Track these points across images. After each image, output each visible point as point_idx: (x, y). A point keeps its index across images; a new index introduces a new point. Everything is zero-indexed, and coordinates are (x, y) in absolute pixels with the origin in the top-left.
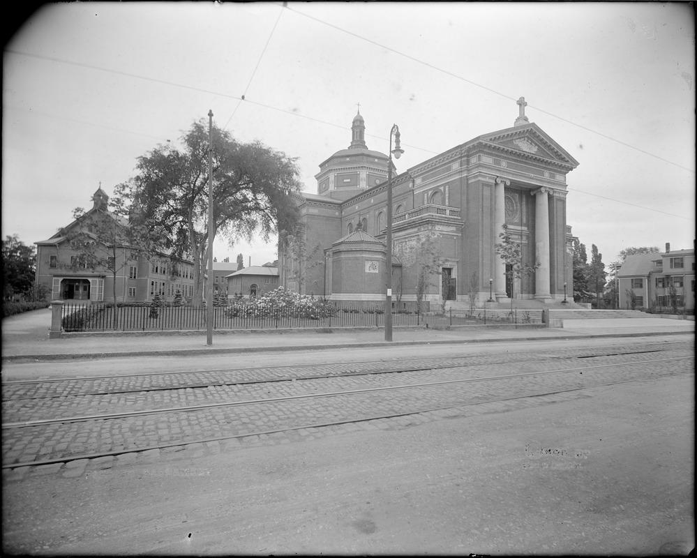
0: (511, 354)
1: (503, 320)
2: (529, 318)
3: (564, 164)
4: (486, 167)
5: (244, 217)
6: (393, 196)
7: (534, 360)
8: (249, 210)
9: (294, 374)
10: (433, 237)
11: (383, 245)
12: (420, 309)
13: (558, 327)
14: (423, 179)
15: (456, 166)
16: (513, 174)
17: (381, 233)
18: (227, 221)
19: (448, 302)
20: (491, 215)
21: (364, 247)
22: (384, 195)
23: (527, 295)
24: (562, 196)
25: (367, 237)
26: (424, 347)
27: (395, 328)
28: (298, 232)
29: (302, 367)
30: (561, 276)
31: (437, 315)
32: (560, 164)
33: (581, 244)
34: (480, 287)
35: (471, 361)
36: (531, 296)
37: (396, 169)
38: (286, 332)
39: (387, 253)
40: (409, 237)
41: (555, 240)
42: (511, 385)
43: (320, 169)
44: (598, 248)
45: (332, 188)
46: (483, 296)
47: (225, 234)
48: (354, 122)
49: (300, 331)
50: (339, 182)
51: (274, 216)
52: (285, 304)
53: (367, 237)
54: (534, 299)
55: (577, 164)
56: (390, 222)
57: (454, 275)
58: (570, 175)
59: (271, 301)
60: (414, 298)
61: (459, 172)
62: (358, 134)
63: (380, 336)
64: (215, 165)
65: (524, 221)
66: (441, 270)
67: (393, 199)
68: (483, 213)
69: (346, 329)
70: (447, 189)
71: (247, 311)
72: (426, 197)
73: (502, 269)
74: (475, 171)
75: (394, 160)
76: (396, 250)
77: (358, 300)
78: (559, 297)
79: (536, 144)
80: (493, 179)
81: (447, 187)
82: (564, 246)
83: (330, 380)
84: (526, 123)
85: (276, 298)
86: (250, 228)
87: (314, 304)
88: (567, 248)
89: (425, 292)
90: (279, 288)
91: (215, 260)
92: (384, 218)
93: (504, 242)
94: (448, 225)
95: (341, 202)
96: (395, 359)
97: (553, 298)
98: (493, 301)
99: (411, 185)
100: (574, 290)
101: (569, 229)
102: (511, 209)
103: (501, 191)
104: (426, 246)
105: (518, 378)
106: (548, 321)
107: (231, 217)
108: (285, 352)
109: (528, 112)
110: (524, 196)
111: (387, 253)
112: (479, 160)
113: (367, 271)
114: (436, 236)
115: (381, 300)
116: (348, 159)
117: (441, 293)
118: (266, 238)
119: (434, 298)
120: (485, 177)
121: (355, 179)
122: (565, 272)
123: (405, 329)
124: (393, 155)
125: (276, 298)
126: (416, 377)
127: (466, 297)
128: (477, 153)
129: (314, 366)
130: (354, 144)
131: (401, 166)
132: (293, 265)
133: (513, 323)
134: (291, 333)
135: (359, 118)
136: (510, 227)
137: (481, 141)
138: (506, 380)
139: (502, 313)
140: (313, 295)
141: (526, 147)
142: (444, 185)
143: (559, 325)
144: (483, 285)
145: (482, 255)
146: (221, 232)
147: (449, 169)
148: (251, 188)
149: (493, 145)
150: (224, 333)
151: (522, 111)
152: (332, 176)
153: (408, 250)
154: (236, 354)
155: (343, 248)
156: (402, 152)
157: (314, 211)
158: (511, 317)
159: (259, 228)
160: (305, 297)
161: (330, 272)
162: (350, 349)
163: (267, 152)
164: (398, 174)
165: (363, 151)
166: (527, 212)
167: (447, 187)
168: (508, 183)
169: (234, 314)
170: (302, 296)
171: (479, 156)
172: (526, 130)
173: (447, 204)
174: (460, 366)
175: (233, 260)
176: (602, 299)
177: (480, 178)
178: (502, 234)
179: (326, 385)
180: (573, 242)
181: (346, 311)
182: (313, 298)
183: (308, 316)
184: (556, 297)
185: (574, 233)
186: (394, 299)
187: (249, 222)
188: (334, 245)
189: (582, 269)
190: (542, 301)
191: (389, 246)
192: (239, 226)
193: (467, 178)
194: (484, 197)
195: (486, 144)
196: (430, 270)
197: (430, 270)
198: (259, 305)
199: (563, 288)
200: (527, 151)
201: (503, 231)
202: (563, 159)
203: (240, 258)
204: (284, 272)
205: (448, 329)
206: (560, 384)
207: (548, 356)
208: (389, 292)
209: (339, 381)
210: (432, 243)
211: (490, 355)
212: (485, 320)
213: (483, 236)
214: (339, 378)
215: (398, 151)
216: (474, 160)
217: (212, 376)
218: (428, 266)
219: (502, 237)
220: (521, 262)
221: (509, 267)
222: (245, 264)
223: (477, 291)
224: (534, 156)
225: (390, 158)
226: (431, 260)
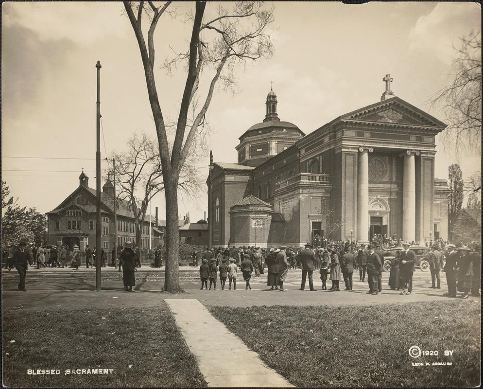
43: (240, 141)
48: (267, 98)
65: (394, 180)
80: (356, 149)
81: (321, 156)
103: (365, 157)
109: (393, 87)
121: (266, 148)
135: (272, 94)
137: (342, 120)
142: (319, 155)
147: (322, 142)
167: (321, 156)
168: (371, 151)
171: (343, 131)
194: (347, 164)
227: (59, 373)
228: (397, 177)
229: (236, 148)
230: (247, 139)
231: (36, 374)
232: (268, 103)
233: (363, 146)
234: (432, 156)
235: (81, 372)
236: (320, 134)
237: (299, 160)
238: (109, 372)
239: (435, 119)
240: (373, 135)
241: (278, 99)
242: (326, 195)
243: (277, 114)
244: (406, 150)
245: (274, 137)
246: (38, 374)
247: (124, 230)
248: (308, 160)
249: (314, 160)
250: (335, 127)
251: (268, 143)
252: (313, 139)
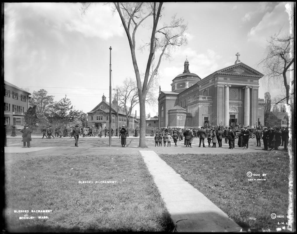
43: (172, 82)
48: (185, 63)
65: (240, 99)
70: (208, 89)
80: (223, 85)
94: (207, 102)
99: (198, 88)
103: (228, 89)
110: (240, 89)
116: (181, 78)
120: (220, 85)
121: (184, 84)
128: (217, 76)
145: (219, 112)
147: (209, 82)
152: (176, 85)
168: (230, 86)
171: (218, 78)
173: (208, 95)
224: (242, 75)
230: (176, 81)
232: (185, 65)
233: (227, 84)
237: (198, 90)
239: (259, 72)
243: (189, 70)
248: (203, 90)
249: (205, 90)
250: (214, 76)
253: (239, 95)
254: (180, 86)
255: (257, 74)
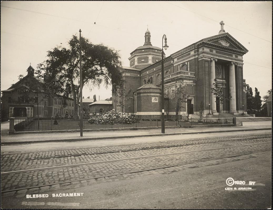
0: (219, 138)
1: (215, 123)
2: (227, 122)
3: (242, 51)
4: (206, 53)
5: (96, 78)
6: (164, 67)
7: (229, 140)
8: (98, 75)
9: (121, 149)
10: (183, 86)
11: (160, 89)
12: (178, 118)
13: (240, 126)
14: (178, 59)
15: (192, 53)
16: (219, 56)
17: (159, 84)
18: (88, 80)
19: (190, 115)
20: (209, 75)
21: (151, 90)
22: (160, 66)
23: (226, 111)
24: (241, 66)
25: (153, 86)
26: (180, 136)
27: (166, 127)
28: (121, 84)
29: (124, 146)
30: (241, 102)
31: (185, 121)
32: (240, 51)
33: (250, 88)
34: (205, 108)
35: (201, 142)
36: (228, 112)
37: (165, 55)
38: (116, 130)
39: (162, 93)
40: (172, 86)
41: (238, 86)
42: (220, 152)
43: (130, 55)
44: (258, 89)
45: (136, 64)
46: (206, 112)
47: (88, 86)
48: (146, 34)
49: (123, 130)
50: (139, 60)
51: (110, 77)
52: (115, 117)
53: (153, 86)
54: (229, 113)
55: (248, 51)
56: (163, 78)
57: (193, 102)
58: (244, 56)
59: (109, 116)
60: (174, 113)
61: (194, 56)
62: (148, 39)
63: (159, 131)
64: (83, 54)
65: (224, 77)
66: (186, 100)
67: (164, 69)
68: (205, 74)
69: (144, 128)
70: (189, 63)
71: (98, 121)
72: (179, 67)
73: (214, 99)
74: (201, 55)
75: (164, 50)
76: (166, 92)
77: (150, 115)
78: (240, 112)
79: (229, 42)
80: (210, 58)
82: (243, 89)
83: (137, 152)
84: (224, 33)
85: (112, 115)
86: (99, 82)
87: (129, 117)
88: (244, 89)
89: (179, 111)
90: (113, 110)
91: (83, 98)
92: (160, 77)
93: (215, 87)
94: (190, 80)
95: (140, 70)
96: (166, 141)
97: (238, 112)
98: (211, 114)
99: (172, 62)
100: (247, 108)
101: (244, 81)
102: (218, 72)
103: (213, 64)
104: (179, 90)
105: (222, 149)
106: (236, 123)
107: (90, 77)
108: (115, 139)
109: (225, 28)
111: (162, 93)
112: (203, 50)
113: (153, 101)
114: (184, 85)
115: (159, 114)
116: (143, 51)
117: (187, 111)
118: (107, 87)
119: (183, 113)
121: (147, 59)
122: (243, 100)
123: (171, 128)
124: (164, 48)
125: (112, 115)
126: (176, 149)
127: (198, 113)
129: (129, 145)
130: (146, 43)
131: (168, 53)
132: (119, 99)
133: (220, 124)
134: (119, 130)
135: (148, 32)
136: (218, 80)
137: (203, 41)
138: (217, 150)
139: (215, 119)
140: (128, 113)
141: (224, 44)
142: (187, 62)
143: (241, 125)
144: (206, 107)
146: (86, 85)
147: (189, 54)
148: (99, 65)
149: (209, 43)
150: (88, 131)
151: (222, 27)
152: (136, 58)
153: (172, 91)
154: (94, 140)
155: (142, 91)
156: (168, 47)
157: (128, 74)
158: (219, 121)
159: (103, 82)
160: (125, 114)
161: (136, 102)
162: (146, 137)
163: (106, 48)
164: (166, 57)
165: (150, 47)
166: (225, 73)
168: (216, 60)
169: (92, 122)
170: (123, 113)
171: (203, 48)
172: (224, 36)
173: (189, 70)
174: (196, 144)
175: (92, 98)
176: (260, 112)
177: (204, 58)
178: (214, 84)
179: (135, 154)
180: (246, 87)
181: (143, 120)
182: (128, 114)
183: (126, 123)
184: (239, 112)
185: (247, 83)
186: (165, 114)
187: (98, 80)
188: (138, 90)
189: (251, 99)
190: (233, 114)
191: (162, 90)
192: (94, 82)
193: (198, 58)
194: (206, 67)
195: (206, 43)
196: (181, 101)
197: (181, 101)
198: (104, 118)
199: (242, 108)
200: (225, 45)
201: (215, 82)
202: (241, 49)
203: (95, 97)
204: (115, 102)
205: (190, 127)
206: (241, 151)
207: (236, 139)
208: (163, 111)
209: (141, 152)
210: (182, 88)
211: (210, 139)
212: (207, 123)
213: (205, 84)
214: (141, 151)
215: (166, 46)
216: (201, 50)
217: (83, 151)
218: (180, 99)
219: (214, 85)
220: (223, 96)
221: (217, 99)
222: (97, 99)
223: (203, 110)
225: (163, 50)
226: (182, 96)
227: (48, 196)
228: (225, 77)
229: (128, 59)
230: (134, 54)
231: (32, 197)
233: (213, 58)
234: (242, 66)
235: (62, 195)
236: (189, 50)
238: (81, 194)
240: (217, 52)
241: (151, 34)
242: (194, 84)
243: (150, 43)
244: (231, 62)
245: (151, 54)
246: (33, 197)
247: (59, 103)
248: (179, 65)
249: (184, 65)
251: (148, 57)
252: (183, 52)
253: (223, 72)
254: (142, 60)
255: (241, 49)
